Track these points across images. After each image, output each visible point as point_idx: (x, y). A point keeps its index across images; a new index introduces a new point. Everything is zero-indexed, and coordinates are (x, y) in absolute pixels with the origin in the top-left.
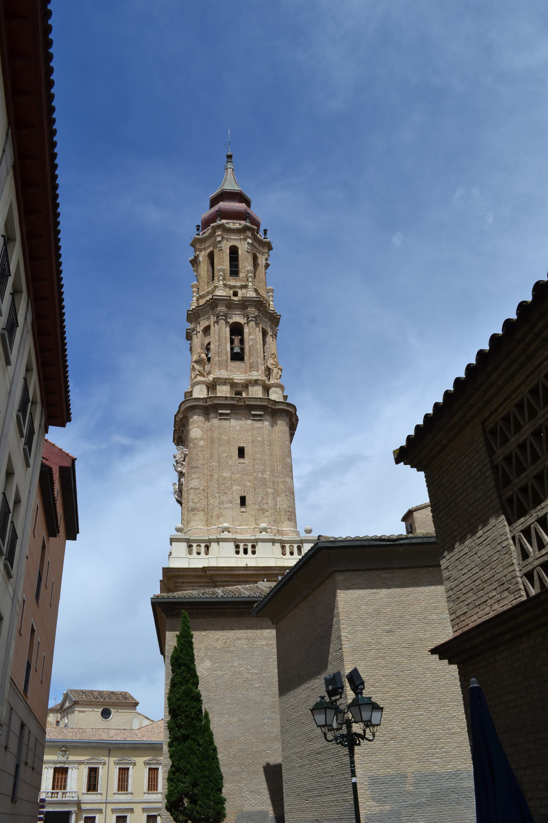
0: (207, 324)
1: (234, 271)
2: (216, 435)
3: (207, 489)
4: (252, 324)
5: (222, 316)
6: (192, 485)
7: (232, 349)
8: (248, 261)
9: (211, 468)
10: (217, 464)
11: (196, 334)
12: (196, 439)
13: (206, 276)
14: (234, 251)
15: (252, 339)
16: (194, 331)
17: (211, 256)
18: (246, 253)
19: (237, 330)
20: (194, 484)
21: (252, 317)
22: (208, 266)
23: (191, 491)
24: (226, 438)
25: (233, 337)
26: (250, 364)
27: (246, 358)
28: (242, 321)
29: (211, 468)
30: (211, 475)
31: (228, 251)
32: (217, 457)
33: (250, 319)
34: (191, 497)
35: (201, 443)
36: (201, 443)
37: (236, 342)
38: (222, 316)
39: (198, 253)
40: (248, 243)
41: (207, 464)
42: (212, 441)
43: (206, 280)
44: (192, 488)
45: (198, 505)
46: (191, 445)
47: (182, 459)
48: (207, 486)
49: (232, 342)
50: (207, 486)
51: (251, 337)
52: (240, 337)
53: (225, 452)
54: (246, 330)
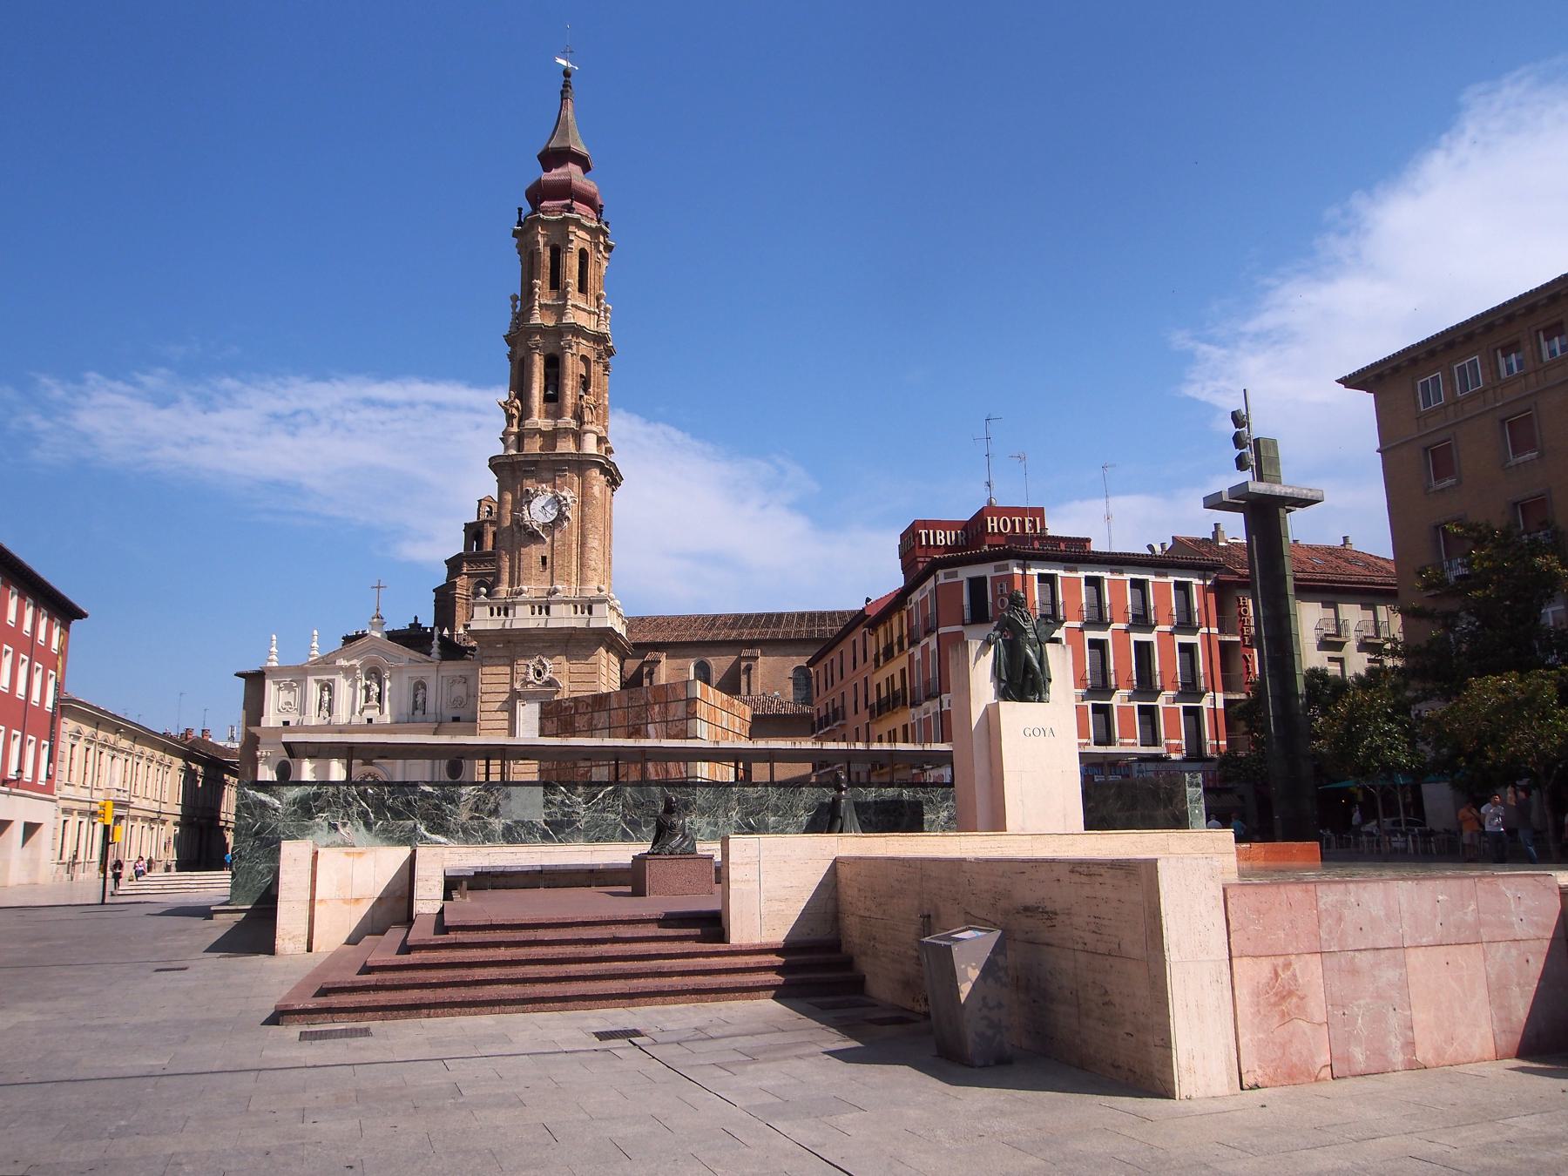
7: (546, 389)
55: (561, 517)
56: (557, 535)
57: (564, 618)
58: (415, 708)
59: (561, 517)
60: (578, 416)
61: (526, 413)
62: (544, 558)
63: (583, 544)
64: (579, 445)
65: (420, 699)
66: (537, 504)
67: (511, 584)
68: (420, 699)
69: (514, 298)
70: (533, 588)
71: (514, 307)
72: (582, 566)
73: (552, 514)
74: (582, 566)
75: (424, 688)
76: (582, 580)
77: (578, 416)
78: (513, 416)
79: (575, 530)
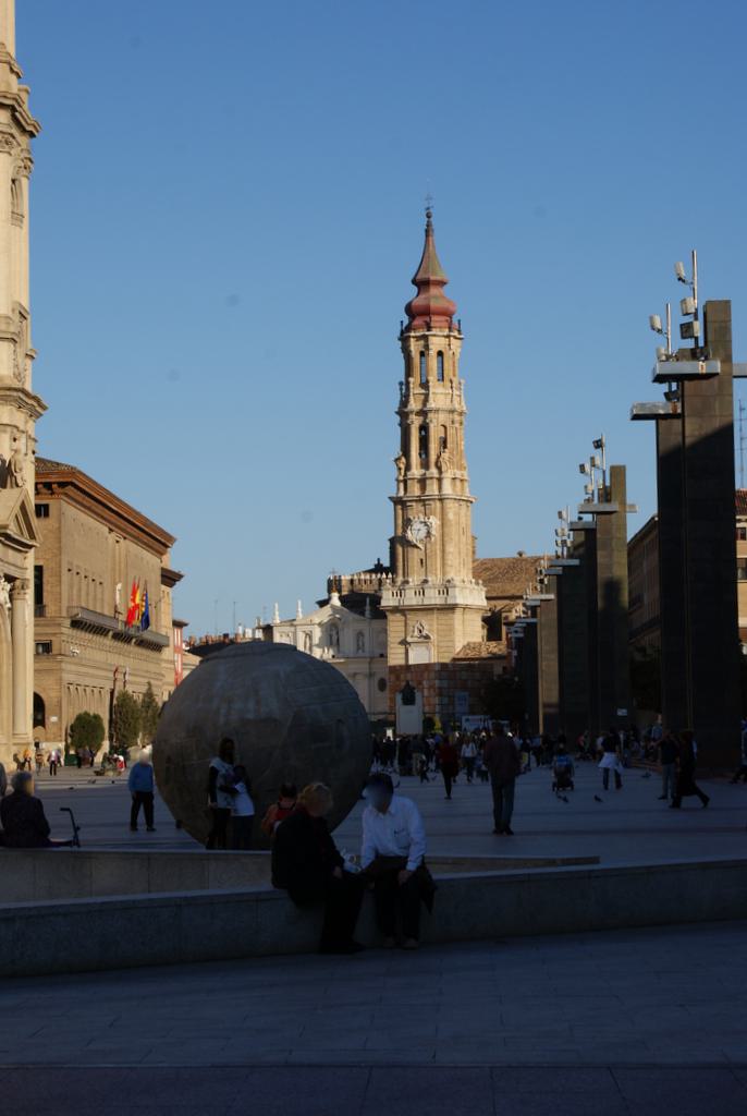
55: (429, 534)
56: (428, 546)
57: (433, 597)
58: (358, 649)
59: (429, 534)
60: (439, 469)
61: (408, 467)
62: (422, 560)
63: (443, 551)
64: (440, 488)
65: (361, 644)
66: (416, 525)
67: (404, 576)
68: (361, 644)
69: (401, 384)
70: (414, 580)
71: (401, 389)
72: (444, 565)
73: (423, 533)
74: (444, 565)
75: (363, 636)
76: (444, 574)
77: (439, 469)
78: (400, 469)
79: (439, 542)
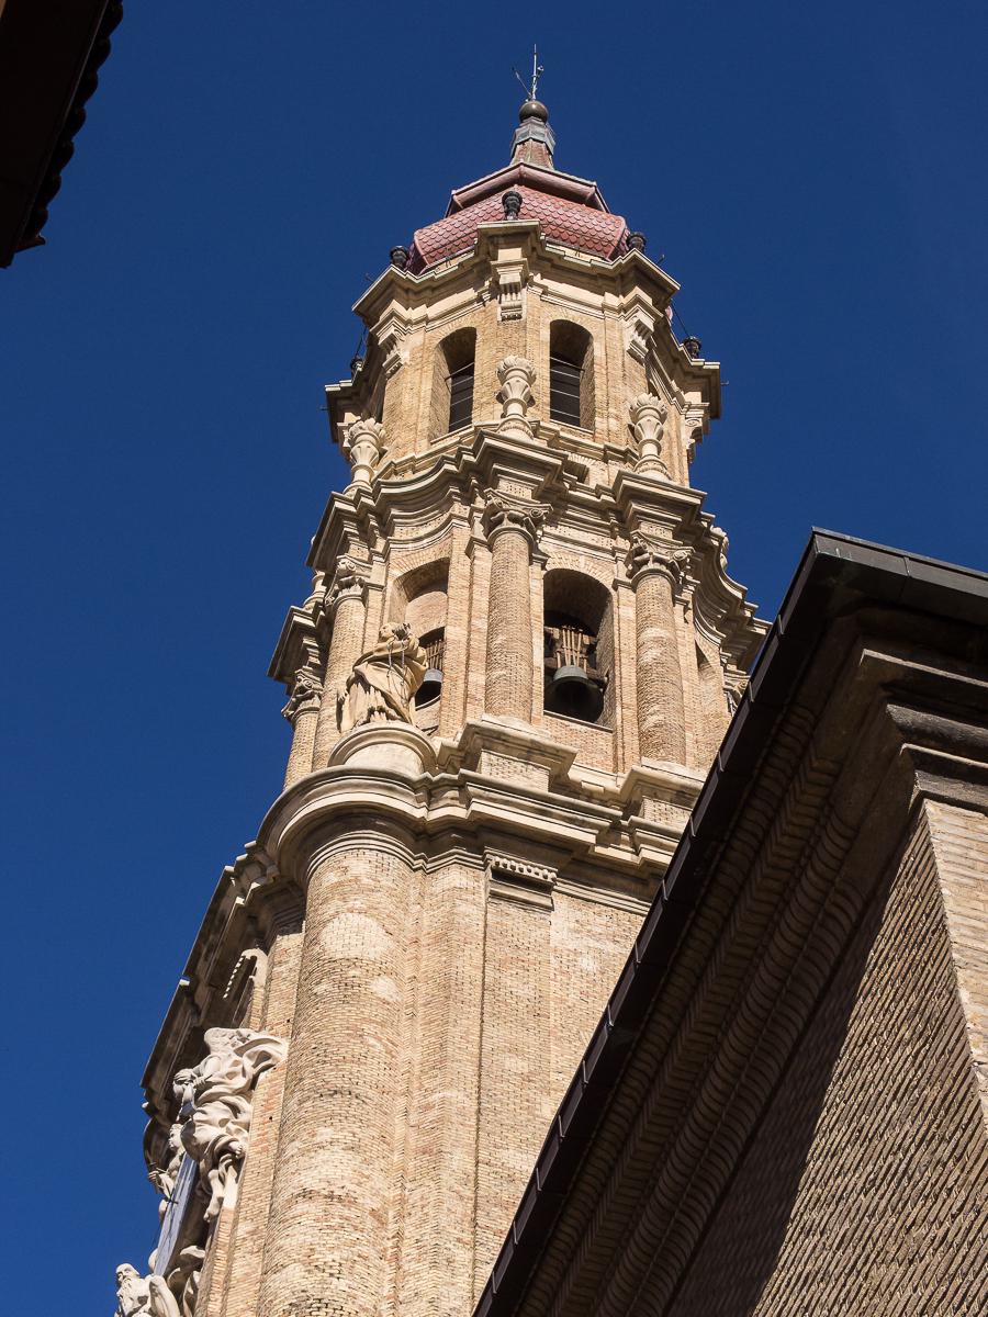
0: (427, 557)
1: (569, 399)
2: (468, 965)
3: (400, 1216)
4: (657, 586)
5: (514, 519)
6: (309, 1180)
7: (550, 672)
8: (631, 386)
9: (432, 1115)
10: (472, 1106)
11: (364, 599)
12: (354, 962)
13: (425, 409)
14: (569, 345)
15: (658, 641)
16: (349, 585)
17: (459, 352)
18: (628, 358)
19: (575, 605)
20: (327, 1171)
21: (661, 561)
22: (435, 383)
23: (301, 1206)
24: (525, 992)
25: (556, 633)
26: (641, 734)
27: (623, 710)
28: (606, 572)
29: (432, 1115)
30: (433, 1153)
31: (546, 334)
32: (471, 1070)
33: (651, 566)
34: (295, 1239)
35: (383, 987)
36: (383, 987)
37: (567, 653)
38: (514, 519)
39: (392, 330)
40: (640, 327)
41: (407, 1093)
42: (447, 988)
43: (424, 425)
44: (307, 1194)
45: (343, 1284)
46: (319, 989)
47: (240, 1082)
48: (402, 1201)
49: (550, 645)
50: (402, 1201)
51: (650, 633)
52: (587, 640)
53: (514, 1050)
54: (624, 607)
